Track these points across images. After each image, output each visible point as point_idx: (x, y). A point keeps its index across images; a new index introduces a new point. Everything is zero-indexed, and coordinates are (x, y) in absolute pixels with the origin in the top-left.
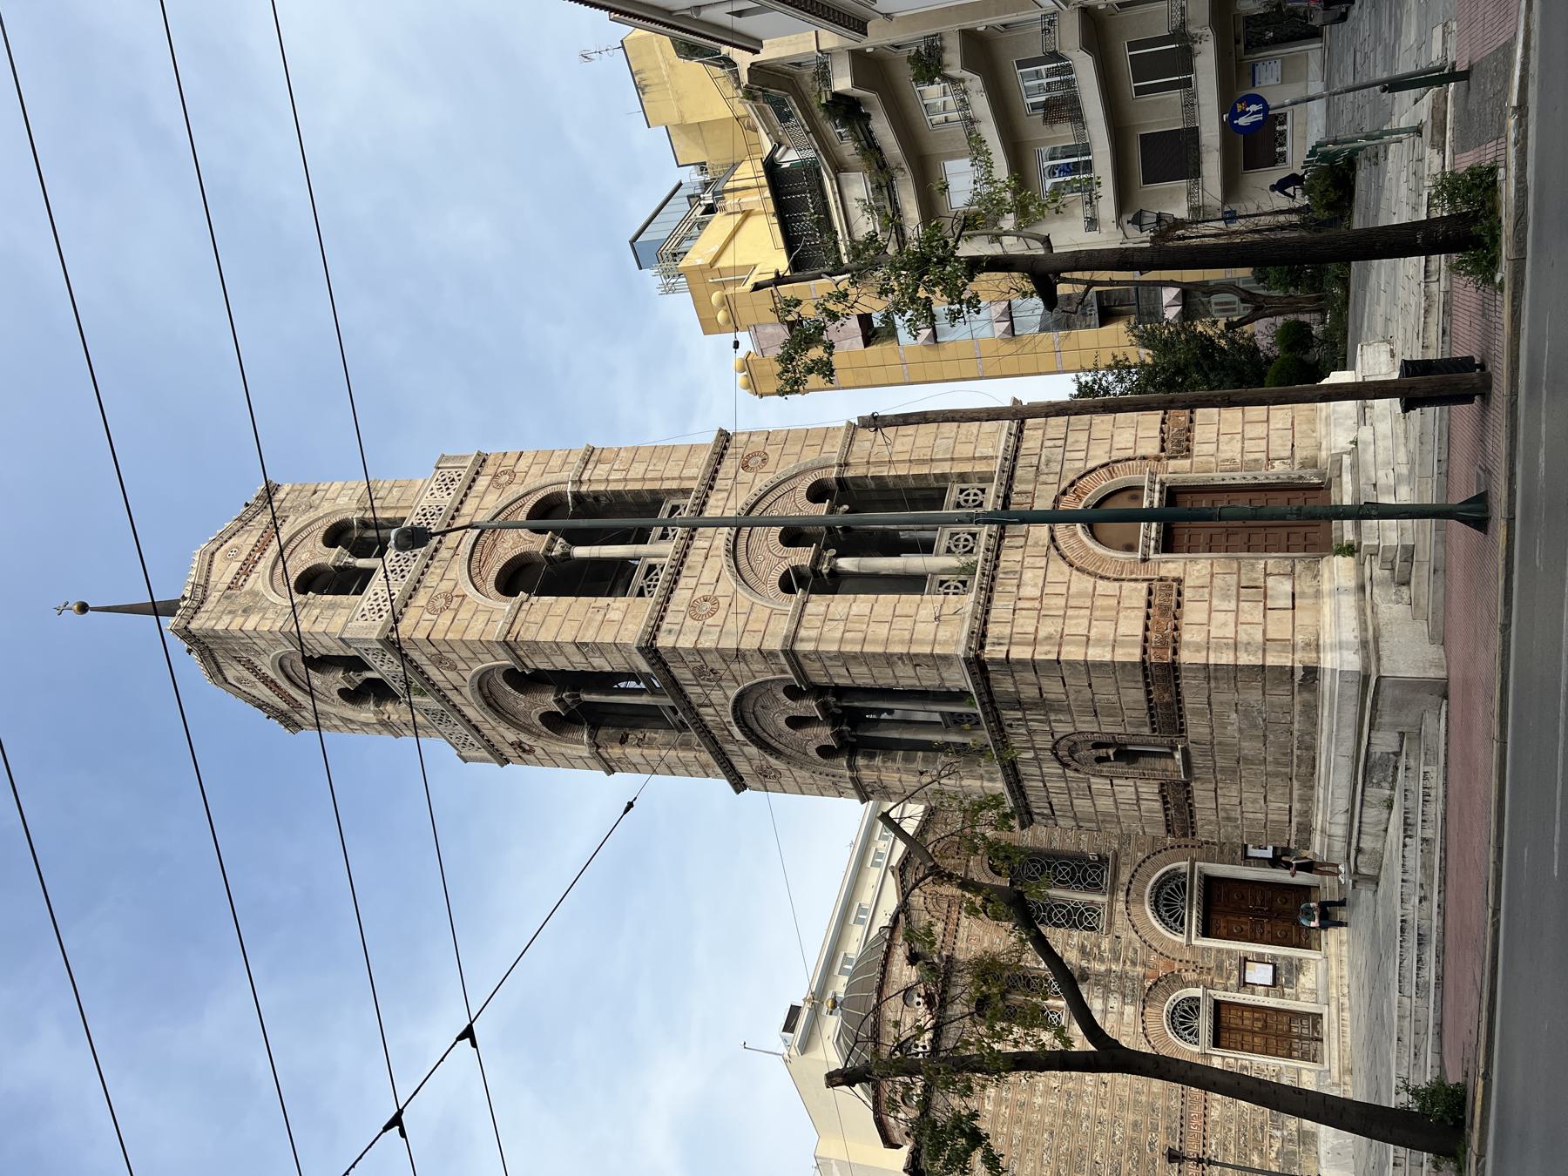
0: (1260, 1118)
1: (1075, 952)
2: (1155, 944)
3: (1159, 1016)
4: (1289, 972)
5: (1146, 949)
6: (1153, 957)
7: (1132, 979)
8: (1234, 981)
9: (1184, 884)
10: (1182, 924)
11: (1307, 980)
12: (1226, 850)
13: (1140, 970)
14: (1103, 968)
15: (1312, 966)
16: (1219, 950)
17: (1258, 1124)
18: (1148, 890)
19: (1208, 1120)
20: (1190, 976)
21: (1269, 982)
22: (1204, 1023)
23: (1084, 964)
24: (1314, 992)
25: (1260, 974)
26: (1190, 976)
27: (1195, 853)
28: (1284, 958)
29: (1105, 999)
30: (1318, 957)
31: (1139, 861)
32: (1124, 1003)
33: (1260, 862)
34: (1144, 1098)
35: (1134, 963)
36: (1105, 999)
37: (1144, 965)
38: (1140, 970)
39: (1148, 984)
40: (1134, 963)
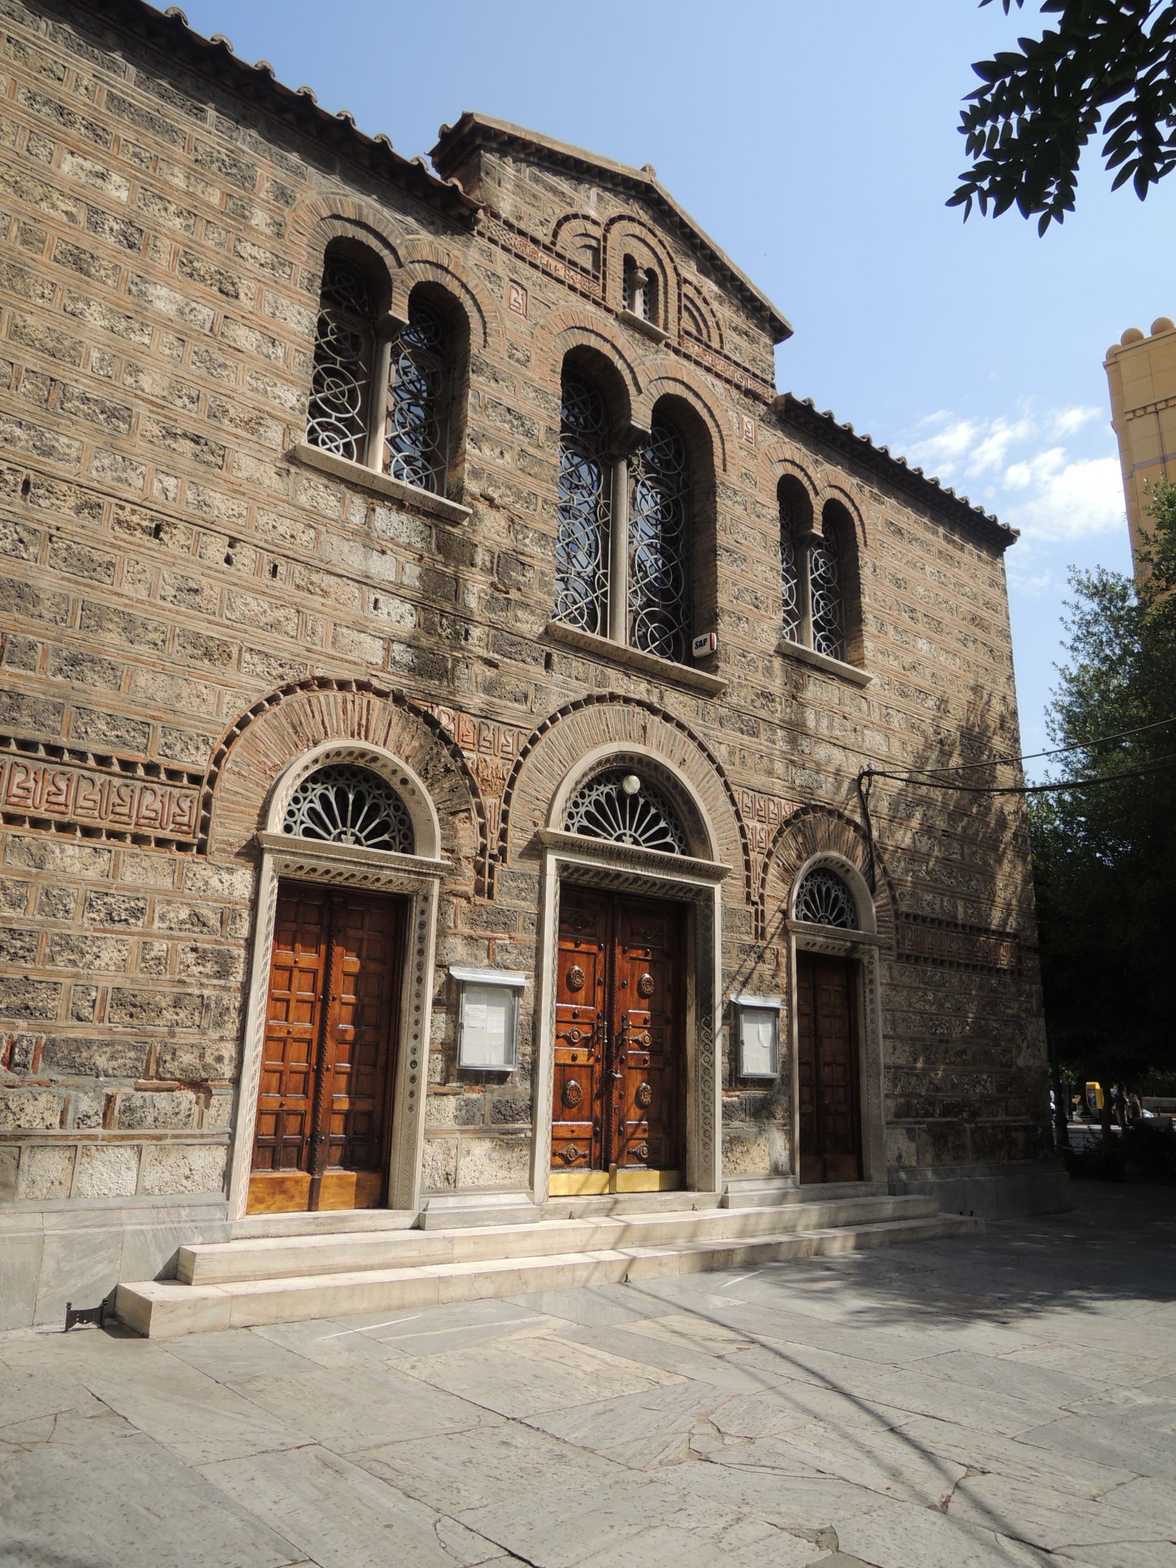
0: (58, 1004)
1: (507, 542)
2: (537, 751)
3: (362, 730)
5: (532, 726)
6: (510, 742)
9: (668, 847)
10: (582, 830)
14: (473, 602)
17: (40, 998)
19: (49, 836)
20: (468, 839)
22: (346, 855)
23: (481, 557)
29: (395, 591)
31: (710, 746)
34: (112, 638)
36: (395, 591)
38: (476, 700)
40: (489, 688)
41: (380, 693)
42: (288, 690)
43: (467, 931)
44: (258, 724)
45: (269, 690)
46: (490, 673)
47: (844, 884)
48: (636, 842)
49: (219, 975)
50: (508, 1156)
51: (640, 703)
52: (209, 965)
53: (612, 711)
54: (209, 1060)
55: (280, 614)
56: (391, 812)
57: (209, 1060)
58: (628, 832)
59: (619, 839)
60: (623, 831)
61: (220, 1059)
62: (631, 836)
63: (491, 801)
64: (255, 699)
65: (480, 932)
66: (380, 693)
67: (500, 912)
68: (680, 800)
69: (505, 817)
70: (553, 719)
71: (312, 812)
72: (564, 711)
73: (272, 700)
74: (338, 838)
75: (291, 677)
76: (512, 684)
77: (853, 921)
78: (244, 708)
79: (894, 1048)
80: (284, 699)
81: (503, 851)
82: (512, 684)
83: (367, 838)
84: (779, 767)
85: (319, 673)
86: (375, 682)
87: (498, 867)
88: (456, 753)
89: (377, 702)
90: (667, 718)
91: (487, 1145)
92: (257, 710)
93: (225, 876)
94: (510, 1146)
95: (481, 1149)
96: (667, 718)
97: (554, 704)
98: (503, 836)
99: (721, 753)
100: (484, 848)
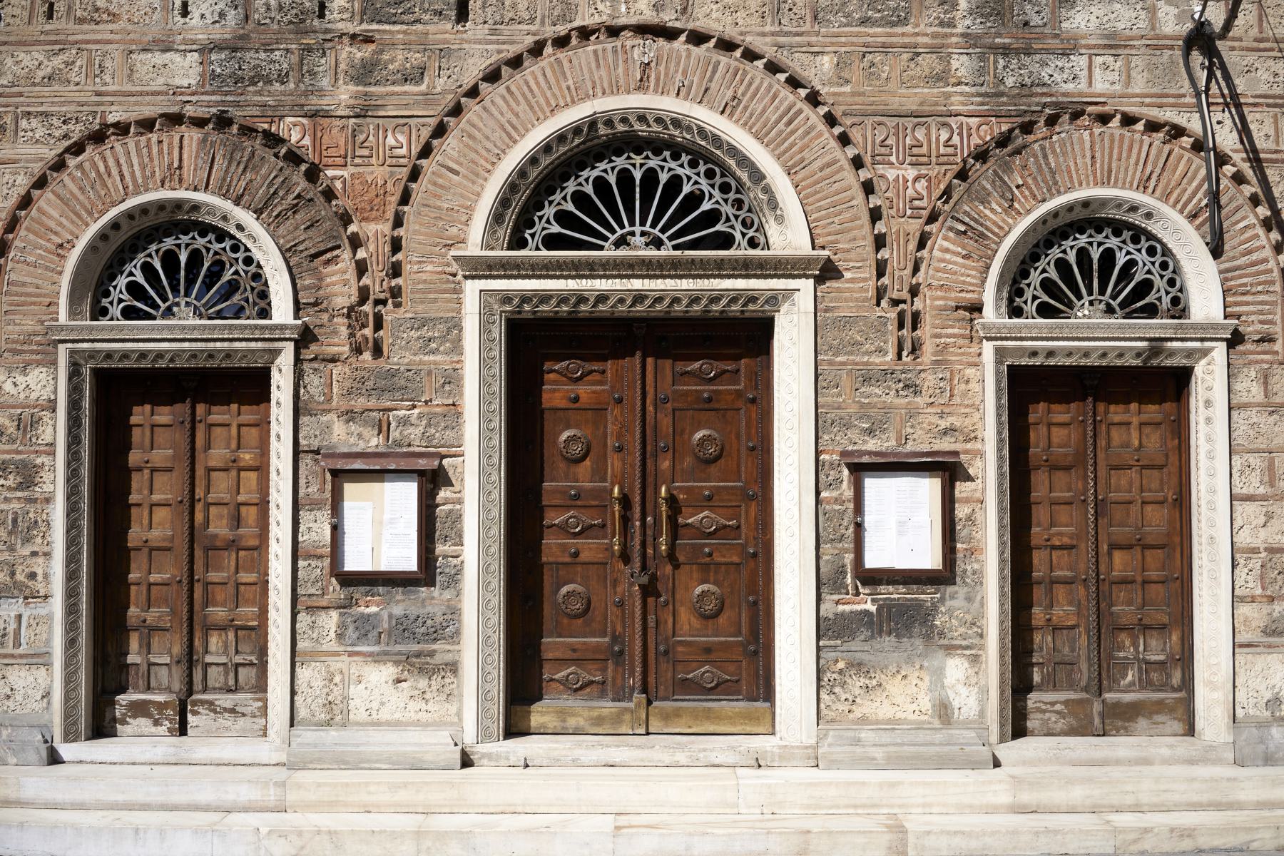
2: (450, 146)
3: (174, 175)
4: (403, 629)
6: (402, 143)
7: (304, 71)
8: (343, 436)
9: (725, 241)
11: (374, 685)
12: (878, 394)
13: (343, 95)
15: (437, 708)
16: (452, 379)
18: (669, 104)
20: (340, 283)
21: (355, 561)
24: (335, 714)
25: (381, 527)
26: (340, 283)
27: (858, 275)
28: (454, 612)
30: (469, 736)
31: (797, 63)
32: (206, 50)
33: (842, 527)
35: (364, 73)
37: (362, 112)
39: (294, 131)
40: (364, 73)
41: (200, 123)
42: (77, 149)
43: (344, 405)
44: (45, 201)
45: (50, 154)
46: (361, 53)
47: (1151, 237)
48: (658, 243)
49: (19, 487)
50: (423, 683)
51: (643, 30)
52: (11, 477)
53: (583, 55)
54: (20, 577)
55: (58, 61)
56: (241, 267)
57: (20, 577)
58: (638, 229)
59: (622, 242)
60: (628, 229)
61: (33, 576)
62: (643, 234)
63: (375, 230)
64: (37, 168)
65: (360, 403)
66: (200, 123)
67: (392, 374)
68: (732, 162)
69: (396, 245)
70: (473, 92)
71: (133, 288)
72: (493, 76)
73: (59, 165)
74: (169, 313)
75: (77, 132)
76: (398, 59)
77: (1175, 301)
78: (23, 182)
79: (1269, 516)
80: (72, 162)
81: (396, 293)
82: (398, 59)
83: (208, 306)
84: (962, 65)
85: (112, 119)
86: (190, 111)
87: (389, 314)
88: (313, 174)
89: (193, 136)
90: (698, 38)
91: (389, 671)
92: (41, 183)
93: (20, 379)
94: (426, 671)
95: (380, 675)
96: (698, 38)
97: (473, 70)
98: (396, 271)
99: (819, 70)
100: (364, 295)
